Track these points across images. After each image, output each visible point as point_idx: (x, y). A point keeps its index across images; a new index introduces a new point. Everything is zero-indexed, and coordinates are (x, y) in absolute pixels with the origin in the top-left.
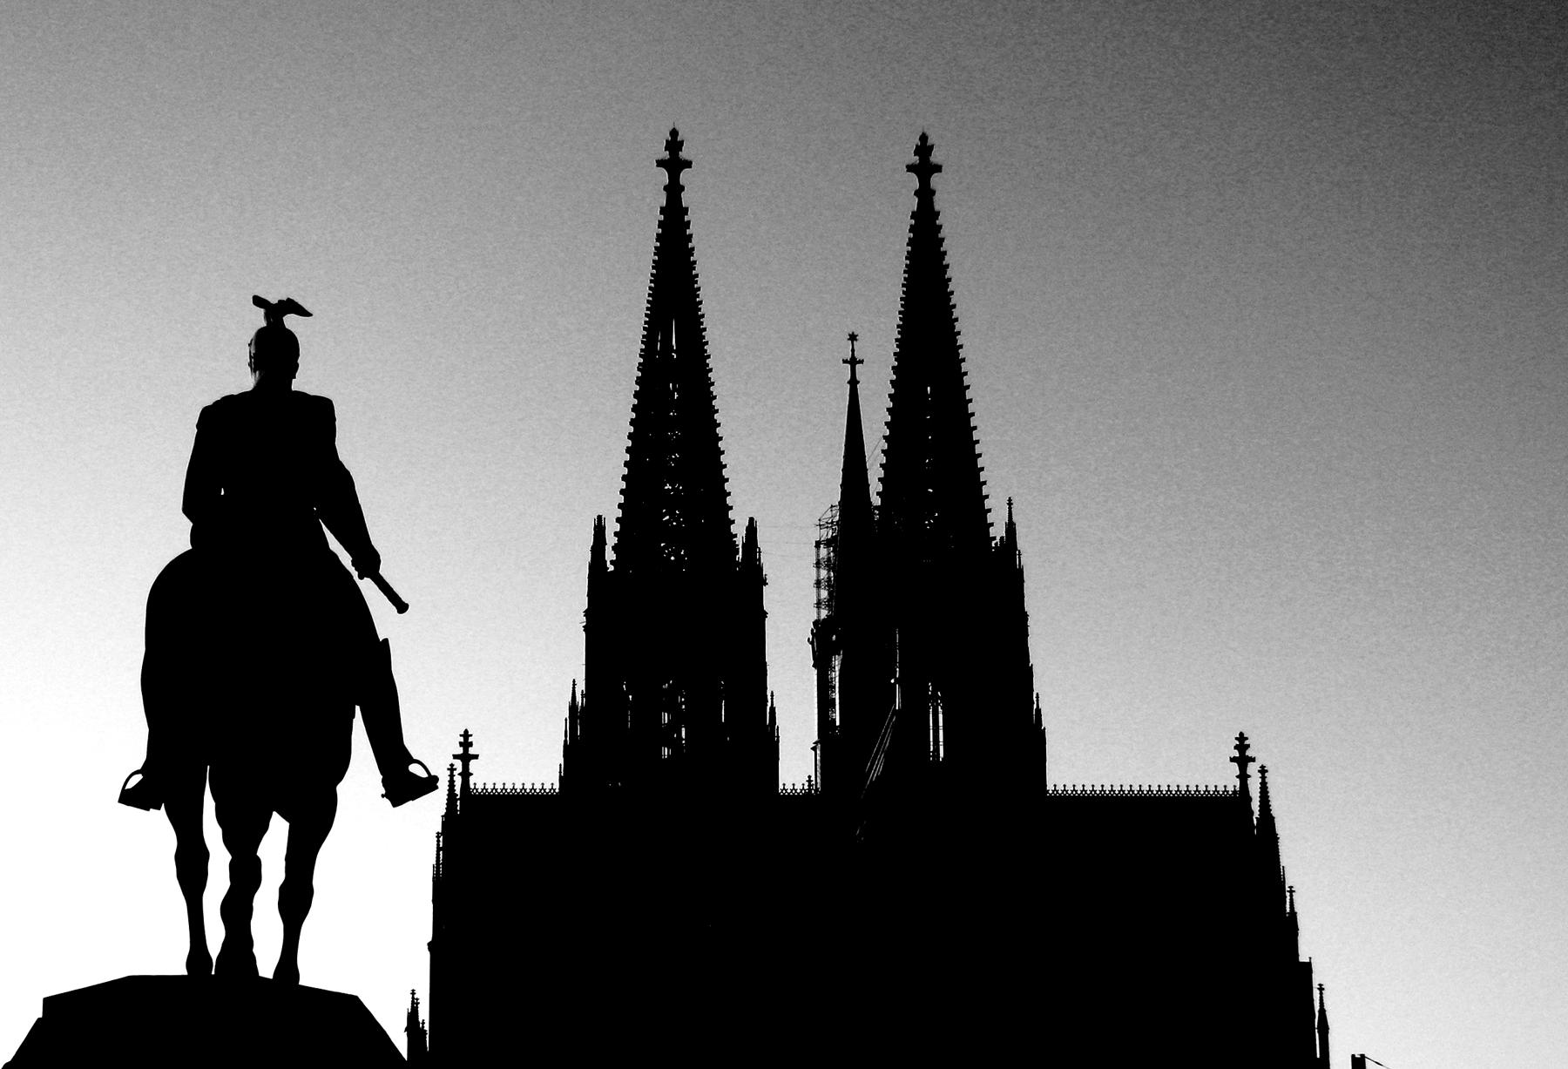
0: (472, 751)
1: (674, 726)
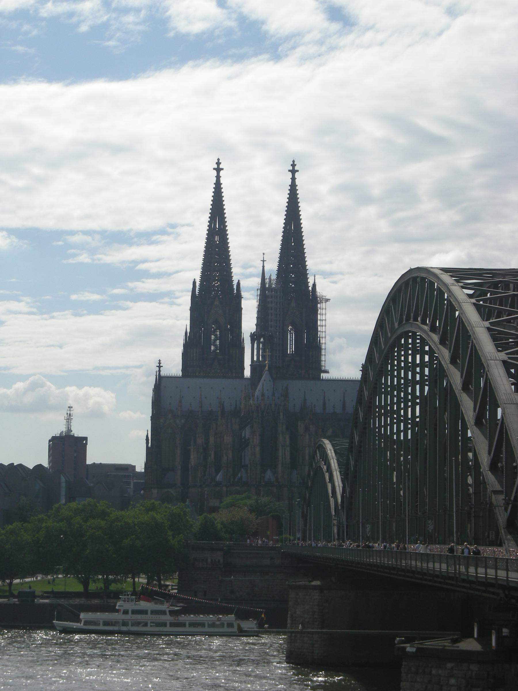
0: (161, 365)
1: (215, 340)
